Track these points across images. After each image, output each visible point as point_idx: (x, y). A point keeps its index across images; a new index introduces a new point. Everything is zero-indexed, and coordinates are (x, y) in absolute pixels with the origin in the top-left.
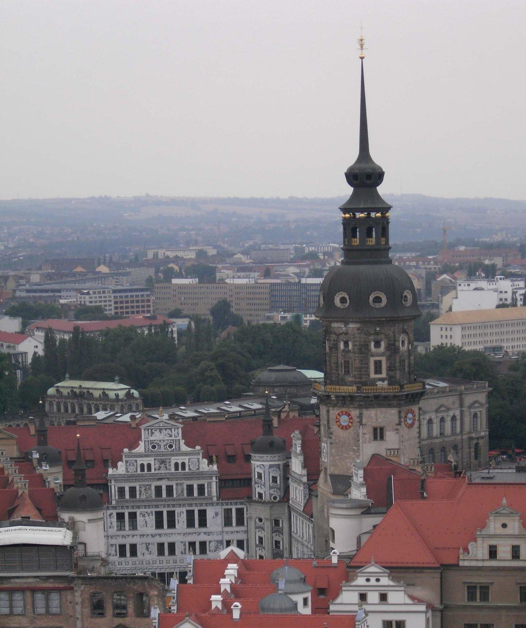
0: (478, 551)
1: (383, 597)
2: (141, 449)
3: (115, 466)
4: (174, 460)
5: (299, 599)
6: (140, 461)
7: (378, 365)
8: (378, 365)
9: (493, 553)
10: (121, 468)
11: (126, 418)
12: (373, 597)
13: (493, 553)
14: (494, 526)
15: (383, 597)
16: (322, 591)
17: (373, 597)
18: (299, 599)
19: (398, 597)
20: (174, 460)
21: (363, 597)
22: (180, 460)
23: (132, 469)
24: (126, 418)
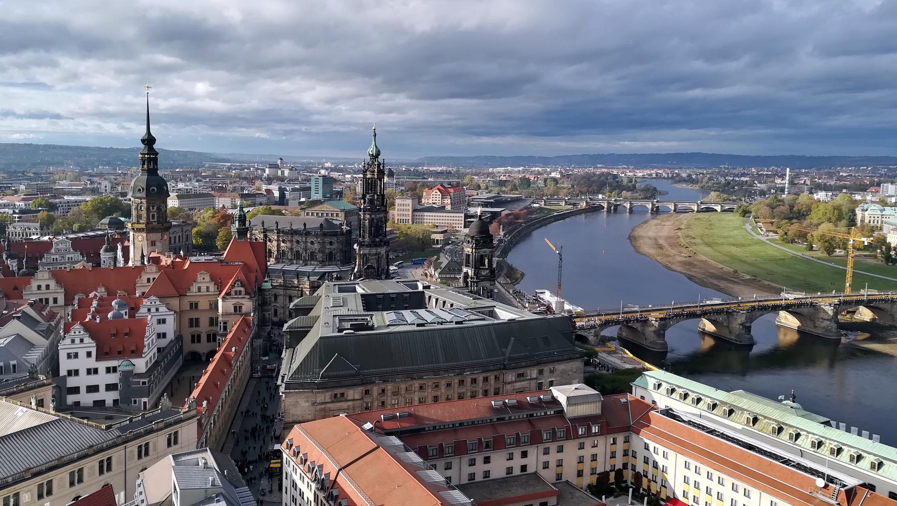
0: (194, 289)
1: (157, 310)
2: (53, 251)
3: (41, 259)
4: (67, 256)
5: (123, 312)
6: (52, 257)
7: (153, 216)
8: (153, 216)
9: (199, 291)
10: (43, 260)
11: (46, 238)
12: (153, 310)
13: (199, 288)
14: (200, 278)
15: (157, 310)
16: (132, 309)
17: (153, 310)
18: (123, 312)
19: (163, 309)
20: (67, 256)
21: (149, 310)
22: (70, 256)
23: (49, 261)
24: (46, 238)
